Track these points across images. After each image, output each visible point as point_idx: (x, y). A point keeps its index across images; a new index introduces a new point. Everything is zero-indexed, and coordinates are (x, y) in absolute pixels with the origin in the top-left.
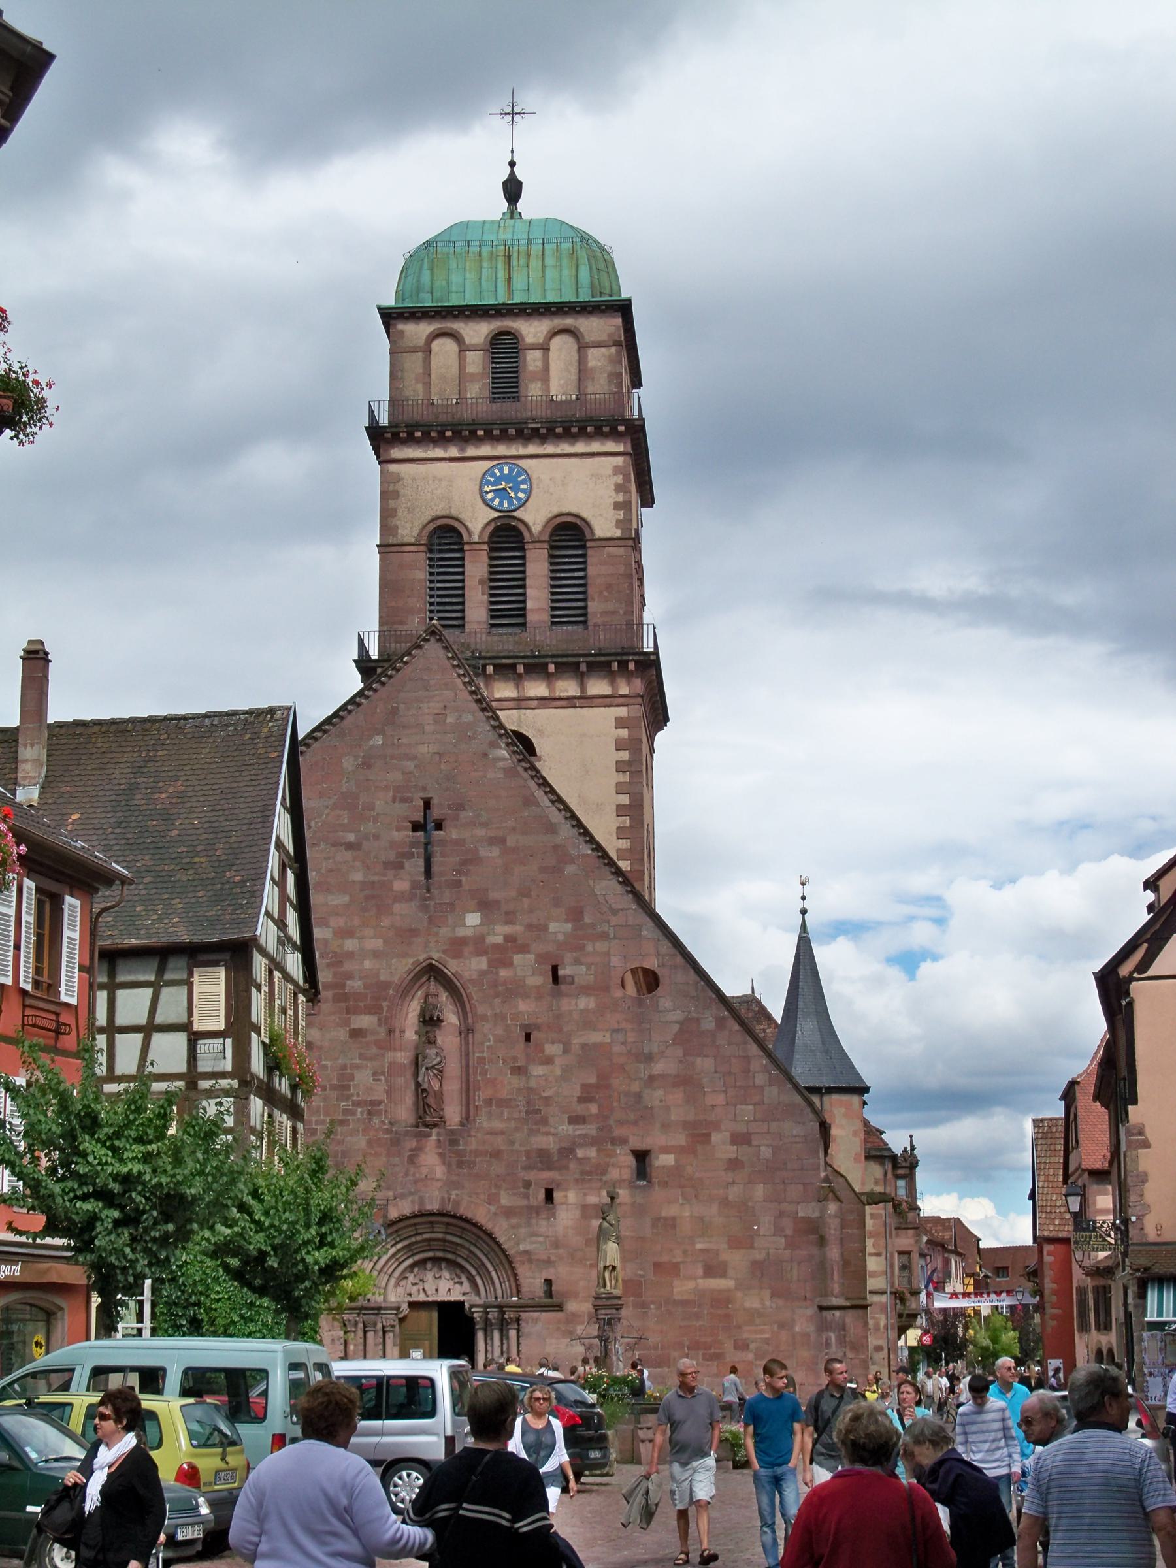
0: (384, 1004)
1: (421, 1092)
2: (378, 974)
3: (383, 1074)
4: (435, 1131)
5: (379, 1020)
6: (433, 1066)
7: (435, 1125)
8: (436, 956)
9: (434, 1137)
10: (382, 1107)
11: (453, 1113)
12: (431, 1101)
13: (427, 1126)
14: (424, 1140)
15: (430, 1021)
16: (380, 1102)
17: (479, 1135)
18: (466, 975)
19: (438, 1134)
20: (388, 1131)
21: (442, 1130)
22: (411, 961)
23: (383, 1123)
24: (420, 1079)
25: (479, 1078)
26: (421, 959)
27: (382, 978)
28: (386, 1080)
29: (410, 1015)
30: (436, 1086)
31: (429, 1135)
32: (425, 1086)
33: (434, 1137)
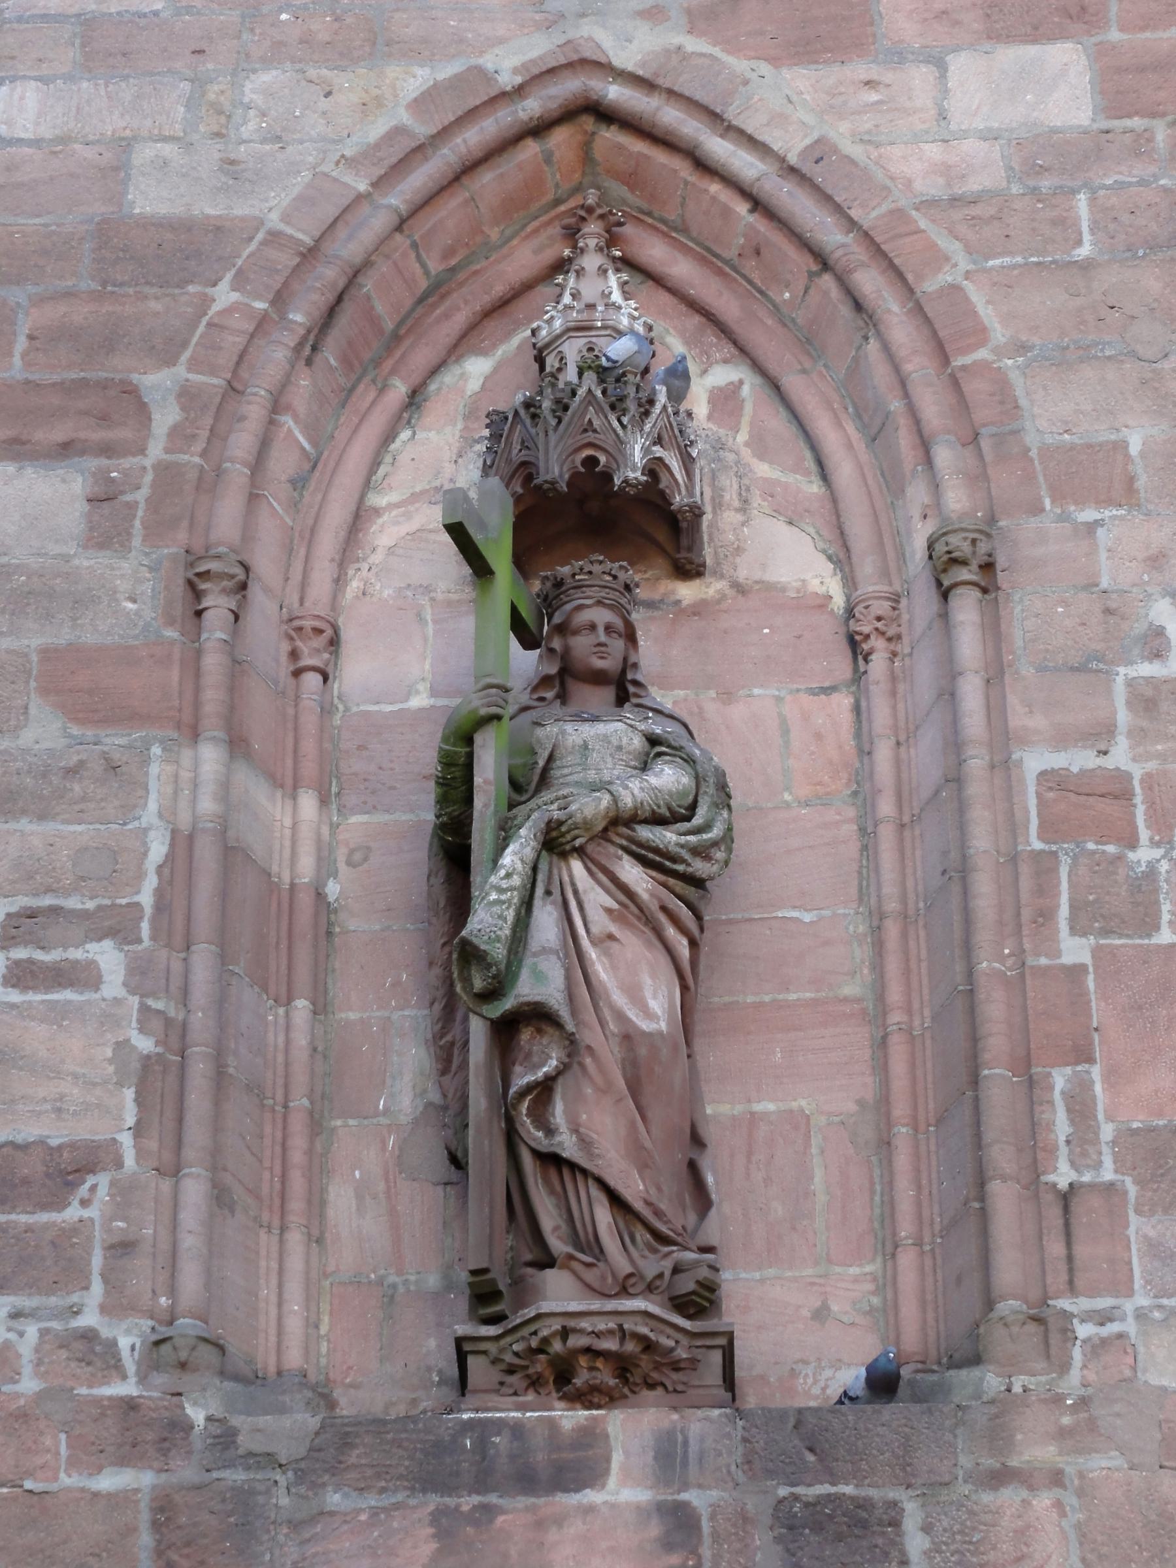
0: (159, 383)
1: (488, 1014)
2: (116, 170)
3: (116, 925)
4: (629, 1431)
5: (103, 497)
6: (620, 822)
7: (634, 1370)
8: (631, 46)
9: (623, 1490)
10: (90, 1208)
11: (807, 1313)
12: (593, 1124)
13: (559, 1371)
14: (515, 1512)
15: (585, 524)
16: (69, 1169)
17: (1102, 1464)
18: (913, 165)
19: (670, 1459)
20: (144, 1432)
21: (703, 1425)
22: (417, 79)
23: (93, 1351)
24: (488, 920)
25: (1075, 950)
26: (506, 64)
27: (149, 198)
28: (139, 975)
29: (385, 534)
30: (638, 990)
31: (577, 1467)
32: (541, 982)
33: (623, 1490)
